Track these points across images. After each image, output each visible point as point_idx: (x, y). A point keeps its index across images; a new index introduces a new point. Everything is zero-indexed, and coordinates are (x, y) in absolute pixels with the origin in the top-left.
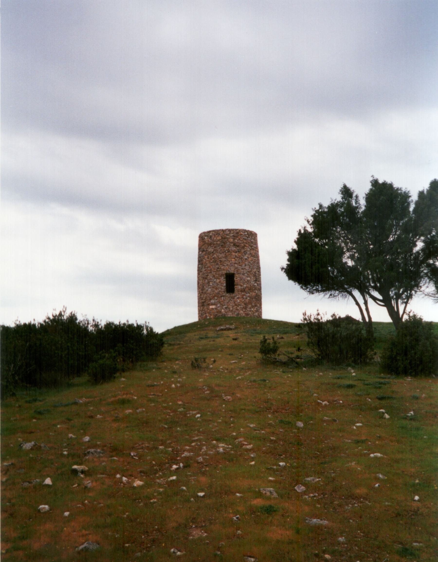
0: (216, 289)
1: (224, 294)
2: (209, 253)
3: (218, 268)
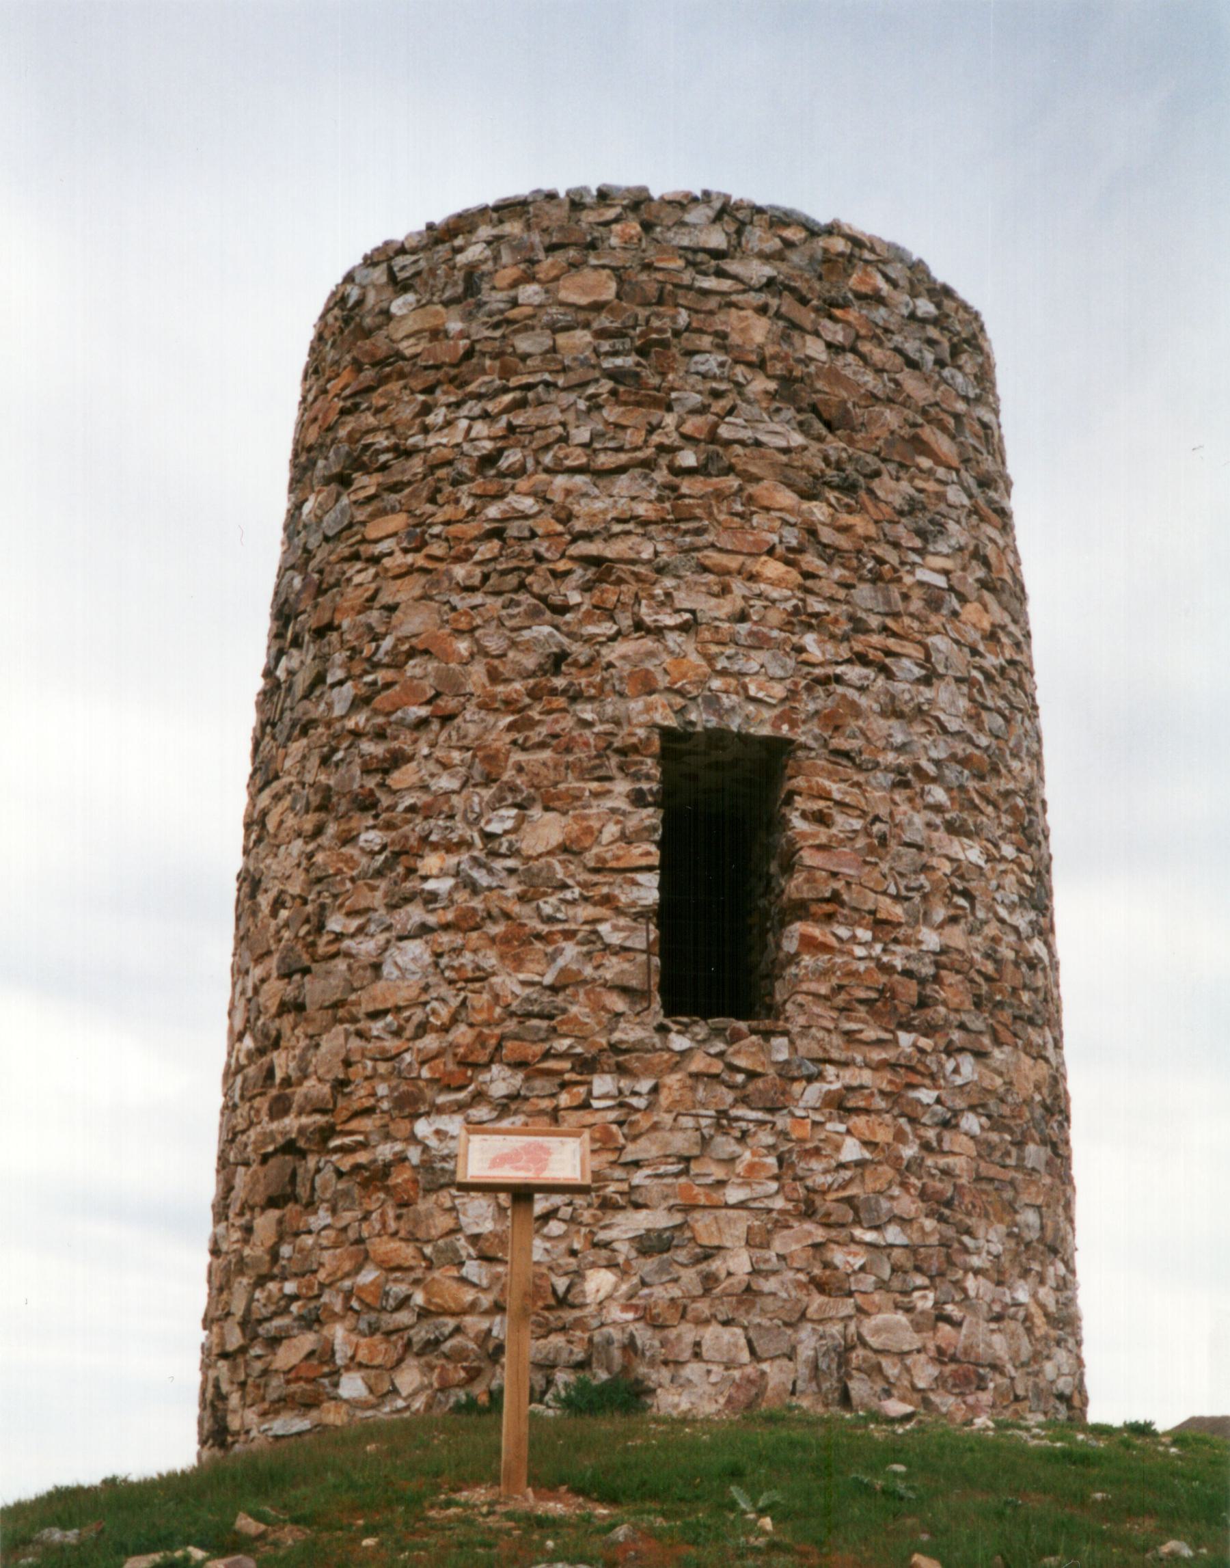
0: (517, 943)
1: (629, 1033)
2: (442, 476)
3: (558, 660)
